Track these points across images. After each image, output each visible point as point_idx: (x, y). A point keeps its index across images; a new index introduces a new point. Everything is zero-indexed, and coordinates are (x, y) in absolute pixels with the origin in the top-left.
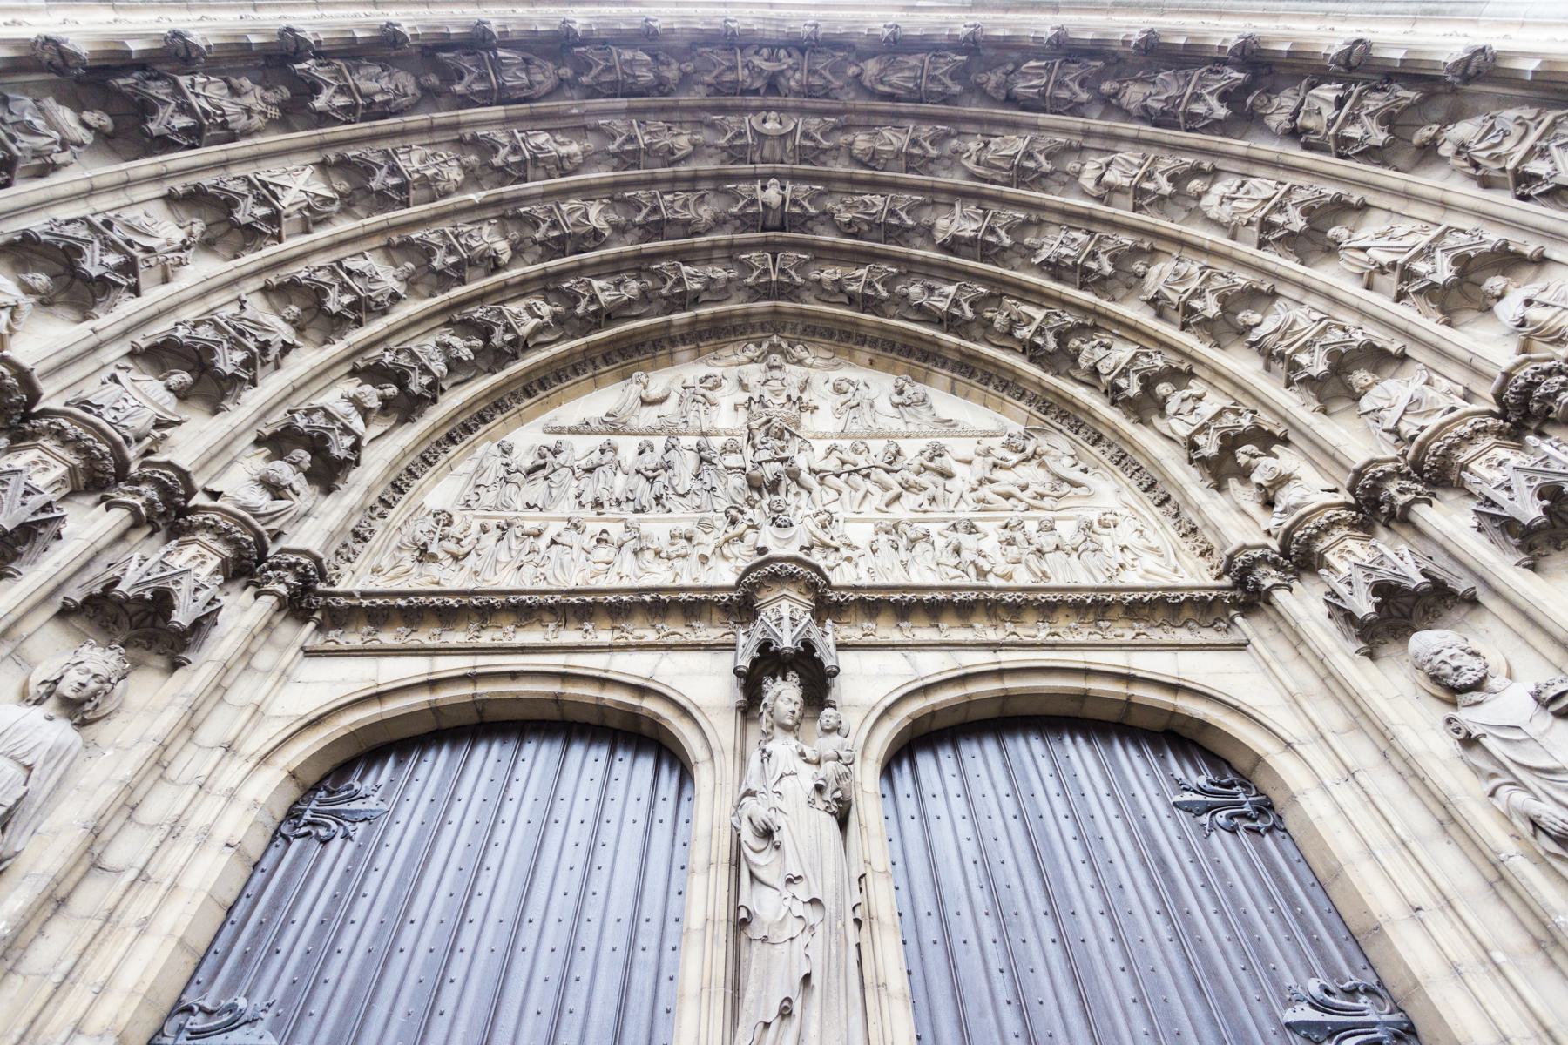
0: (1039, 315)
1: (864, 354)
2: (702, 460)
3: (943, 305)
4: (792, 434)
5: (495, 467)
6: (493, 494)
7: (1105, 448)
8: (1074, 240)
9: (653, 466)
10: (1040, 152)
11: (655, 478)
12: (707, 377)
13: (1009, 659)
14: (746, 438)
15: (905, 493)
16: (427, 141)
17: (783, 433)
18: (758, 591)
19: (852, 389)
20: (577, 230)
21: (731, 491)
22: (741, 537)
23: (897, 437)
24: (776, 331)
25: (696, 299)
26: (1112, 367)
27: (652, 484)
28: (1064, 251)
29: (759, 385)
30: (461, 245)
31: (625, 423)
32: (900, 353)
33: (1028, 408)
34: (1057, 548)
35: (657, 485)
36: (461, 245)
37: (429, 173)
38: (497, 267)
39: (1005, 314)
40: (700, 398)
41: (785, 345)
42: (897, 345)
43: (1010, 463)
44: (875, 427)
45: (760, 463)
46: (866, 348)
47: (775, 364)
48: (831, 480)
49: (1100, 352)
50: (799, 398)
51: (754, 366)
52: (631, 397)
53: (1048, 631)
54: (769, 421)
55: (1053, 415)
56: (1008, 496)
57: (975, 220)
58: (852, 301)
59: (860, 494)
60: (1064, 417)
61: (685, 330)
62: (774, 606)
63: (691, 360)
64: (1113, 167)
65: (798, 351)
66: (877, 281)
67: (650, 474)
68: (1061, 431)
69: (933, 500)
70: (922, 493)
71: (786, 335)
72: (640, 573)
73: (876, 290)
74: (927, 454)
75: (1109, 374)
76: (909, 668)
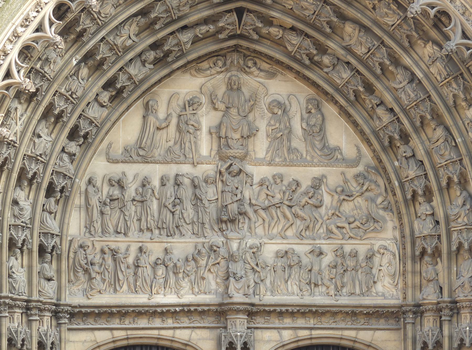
11: (174, 212)
13: (315, 333)
30: (73, 98)
34: (353, 269)
35: (177, 216)
41: (242, 62)
45: (226, 206)
48: (262, 213)
51: (221, 76)
53: (332, 321)
58: (288, 54)
62: (234, 320)
70: (304, 221)
74: (310, 195)
76: (279, 337)
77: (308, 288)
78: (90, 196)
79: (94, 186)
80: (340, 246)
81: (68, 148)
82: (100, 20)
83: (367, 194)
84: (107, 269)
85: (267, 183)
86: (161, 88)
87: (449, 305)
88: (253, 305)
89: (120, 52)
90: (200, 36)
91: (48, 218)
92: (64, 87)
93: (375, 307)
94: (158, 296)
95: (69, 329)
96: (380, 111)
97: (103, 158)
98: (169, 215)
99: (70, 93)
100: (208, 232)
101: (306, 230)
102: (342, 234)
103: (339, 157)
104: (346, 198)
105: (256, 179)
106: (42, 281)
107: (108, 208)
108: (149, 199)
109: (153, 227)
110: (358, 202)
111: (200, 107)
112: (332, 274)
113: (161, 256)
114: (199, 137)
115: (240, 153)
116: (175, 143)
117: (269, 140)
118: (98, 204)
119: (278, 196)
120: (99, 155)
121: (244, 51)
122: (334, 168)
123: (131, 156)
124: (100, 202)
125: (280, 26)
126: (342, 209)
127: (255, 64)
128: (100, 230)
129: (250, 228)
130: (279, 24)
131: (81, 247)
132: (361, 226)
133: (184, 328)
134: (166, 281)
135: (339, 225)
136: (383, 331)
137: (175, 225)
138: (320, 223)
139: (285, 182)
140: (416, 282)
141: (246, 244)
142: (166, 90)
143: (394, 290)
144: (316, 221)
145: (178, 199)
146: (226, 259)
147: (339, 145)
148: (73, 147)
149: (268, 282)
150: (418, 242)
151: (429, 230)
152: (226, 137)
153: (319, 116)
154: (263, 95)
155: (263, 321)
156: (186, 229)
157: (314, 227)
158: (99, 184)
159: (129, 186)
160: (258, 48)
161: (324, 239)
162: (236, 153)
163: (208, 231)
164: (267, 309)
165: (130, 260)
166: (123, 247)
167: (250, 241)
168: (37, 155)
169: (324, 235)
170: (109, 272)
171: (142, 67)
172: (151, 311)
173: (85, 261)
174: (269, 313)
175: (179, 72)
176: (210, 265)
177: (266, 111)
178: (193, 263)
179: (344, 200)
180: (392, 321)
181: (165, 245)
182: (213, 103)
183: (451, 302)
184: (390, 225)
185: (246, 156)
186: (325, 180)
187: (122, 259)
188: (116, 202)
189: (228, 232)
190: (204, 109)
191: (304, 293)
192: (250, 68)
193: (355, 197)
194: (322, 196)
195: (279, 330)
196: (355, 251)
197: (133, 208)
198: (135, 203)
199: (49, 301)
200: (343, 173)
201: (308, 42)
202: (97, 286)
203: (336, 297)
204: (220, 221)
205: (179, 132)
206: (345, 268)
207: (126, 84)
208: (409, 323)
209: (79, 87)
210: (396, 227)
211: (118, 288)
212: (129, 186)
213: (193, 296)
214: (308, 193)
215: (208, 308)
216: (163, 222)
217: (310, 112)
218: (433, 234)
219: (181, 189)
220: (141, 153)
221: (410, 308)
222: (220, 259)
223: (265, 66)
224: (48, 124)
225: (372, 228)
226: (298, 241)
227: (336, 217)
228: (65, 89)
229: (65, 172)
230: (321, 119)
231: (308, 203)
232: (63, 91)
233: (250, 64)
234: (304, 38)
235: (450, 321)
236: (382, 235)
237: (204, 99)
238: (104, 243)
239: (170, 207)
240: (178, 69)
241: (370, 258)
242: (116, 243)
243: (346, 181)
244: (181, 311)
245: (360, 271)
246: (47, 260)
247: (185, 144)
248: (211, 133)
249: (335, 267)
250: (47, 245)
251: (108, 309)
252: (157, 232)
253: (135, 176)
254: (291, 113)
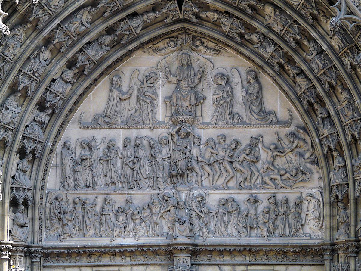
1: (233, 52)
5: (68, 161)
6: (72, 179)
30: (35, 76)
34: (283, 214)
35: (135, 172)
36: (35, 76)
48: (207, 168)
51: (175, 54)
52: (115, 101)
59: (216, 177)
70: (243, 174)
74: (247, 152)
77: (245, 230)
78: (64, 157)
79: (68, 149)
80: (273, 194)
81: (37, 117)
82: (50, 10)
83: (297, 150)
84: (77, 217)
85: (212, 143)
86: (124, 66)
87: (353, 243)
88: (196, 245)
89: (75, 37)
90: (148, 21)
91: (21, 175)
92: (28, 67)
93: (300, 246)
94: (119, 238)
95: (45, 267)
96: (299, 80)
97: (76, 125)
98: (130, 172)
99: (32, 72)
100: (162, 185)
102: (275, 184)
103: (274, 119)
104: (278, 154)
105: (203, 140)
106: (16, 226)
107: (79, 166)
108: (113, 158)
109: (116, 181)
110: (290, 157)
111: (157, 81)
112: (265, 218)
113: (123, 205)
114: (156, 106)
115: (188, 119)
116: (136, 111)
117: (215, 106)
118: (71, 163)
119: (221, 153)
120: (73, 123)
121: (192, 33)
122: (270, 129)
123: (98, 123)
124: (74, 162)
125: (216, 10)
126: (276, 163)
127: (202, 43)
128: (72, 185)
129: (197, 181)
130: (215, 9)
131: (56, 199)
132: (291, 178)
133: (139, 265)
134: (125, 227)
135: (272, 176)
136: (310, 267)
138: (256, 176)
139: (228, 142)
140: (334, 224)
141: (193, 194)
142: (129, 67)
143: (319, 232)
144: (253, 174)
145: (137, 158)
146: (176, 207)
147: (274, 109)
148: (43, 117)
149: (212, 226)
150: (334, 190)
151: (341, 179)
152: (176, 105)
153: (256, 85)
154: (210, 69)
155: (206, 258)
156: (144, 182)
157: (250, 179)
158: (72, 146)
159: (98, 148)
160: (200, 29)
161: (259, 189)
163: (162, 184)
164: (208, 248)
165: (98, 209)
166: (91, 198)
167: (196, 192)
168: (5, 124)
169: (259, 186)
171: (100, 49)
172: (111, 251)
173: (59, 210)
174: (211, 252)
175: (138, 53)
176: (162, 212)
177: (212, 82)
178: (148, 211)
179: (277, 155)
180: (317, 258)
181: (126, 196)
182: (168, 78)
183: (356, 241)
184: (316, 176)
185: (194, 121)
186: (261, 139)
187: (90, 209)
188: (86, 161)
189: (177, 185)
190: (160, 82)
191: (241, 235)
192: (198, 46)
193: (286, 153)
194: (259, 153)
195: (220, 266)
196: (285, 199)
197: (101, 166)
198: (102, 162)
199: (20, 243)
200: (277, 133)
201: (238, 22)
202: (68, 231)
203: (268, 238)
204: (171, 176)
205: (139, 102)
206: (277, 213)
207: (85, 63)
208: (327, 259)
209: (40, 67)
210: (321, 178)
211: (85, 232)
212: (98, 148)
213: (148, 238)
214: (246, 150)
215: (158, 248)
216: (124, 177)
217: (249, 82)
218: (344, 183)
219: (139, 149)
220: (107, 120)
221: (327, 247)
222: (170, 207)
223: (211, 45)
224: (16, 97)
225: (301, 179)
226: (238, 191)
227: (270, 170)
228: (29, 69)
229: (34, 138)
230: (257, 87)
232: (26, 70)
233: (198, 43)
234: (234, 20)
235: (355, 257)
236: (309, 185)
237: (160, 74)
238: (76, 195)
239: (131, 164)
240: (137, 48)
241: (299, 205)
242: (86, 195)
243: (279, 139)
244: (136, 251)
245: (290, 217)
246: (20, 210)
247: (143, 112)
248: (166, 103)
249: (268, 212)
250: (18, 197)
251: (75, 250)
252: (120, 185)
253: (103, 139)
254: (233, 84)
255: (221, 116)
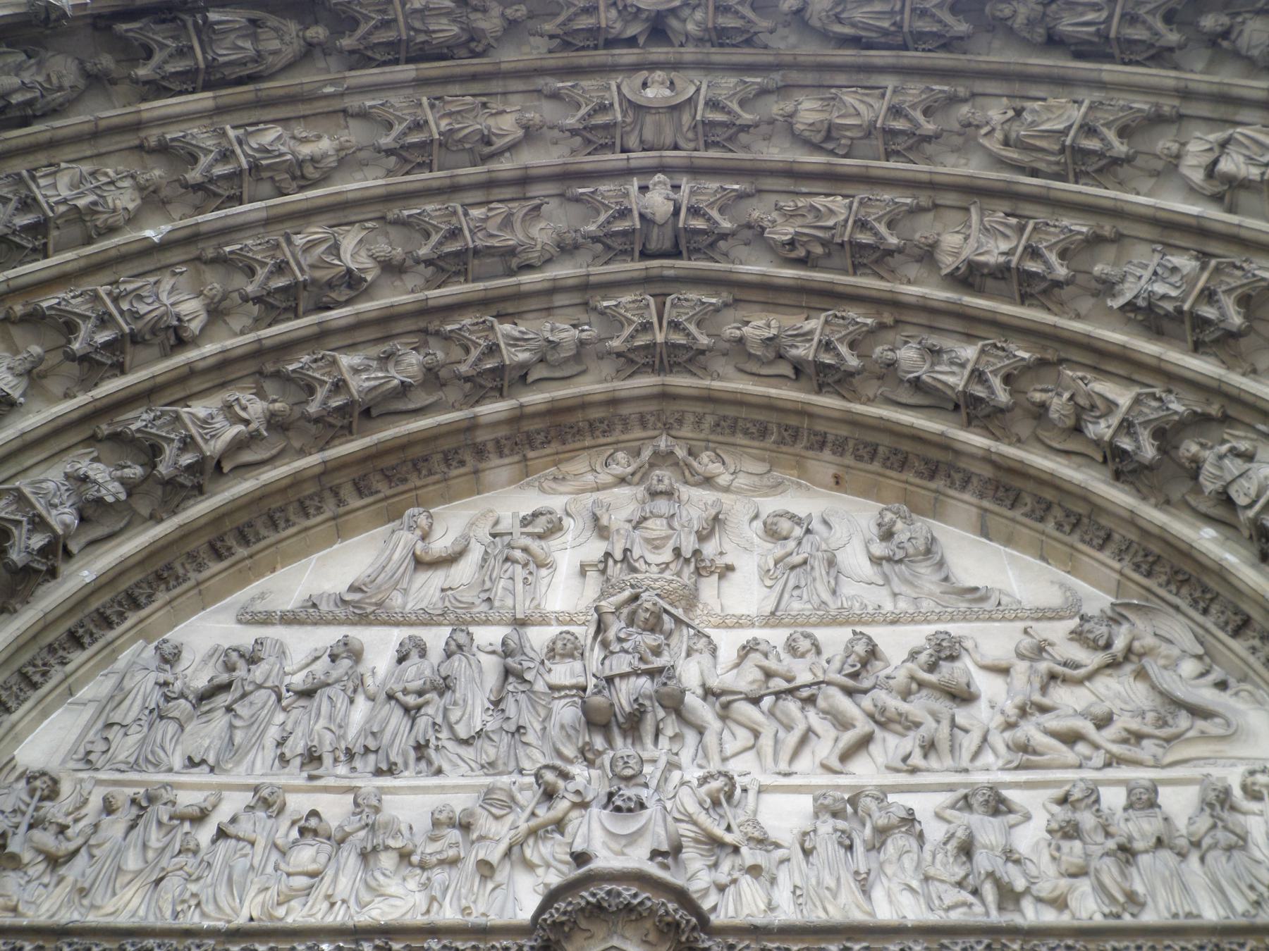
0: (1123, 397)
1: (824, 465)
2: (507, 672)
3: (956, 380)
4: (678, 621)
5: (144, 686)
6: (134, 739)
7: (1257, 642)
8: (1174, 270)
9: (417, 684)
10: (1108, 125)
11: (419, 708)
12: (535, 515)
14: (592, 630)
15: (879, 733)
16: (88, 153)
17: (659, 618)
18: (568, 937)
19: (798, 532)
20: (318, 274)
21: (554, 731)
22: (559, 825)
23: (873, 622)
24: (667, 427)
25: (524, 378)
26: (1253, 492)
27: (414, 720)
28: (1160, 288)
29: (629, 526)
30: (122, 312)
31: (379, 604)
32: (886, 463)
33: (1117, 565)
34: (1159, 842)
35: (422, 722)
37: (81, 203)
38: (178, 338)
39: (1066, 395)
40: (518, 554)
42: (881, 450)
43: (1081, 672)
44: (833, 605)
45: (610, 680)
46: (827, 454)
47: (661, 487)
48: (744, 709)
49: (1233, 466)
50: (696, 553)
51: (625, 491)
52: (396, 556)
54: (636, 598)
55: (1163, 578)
56: (1071, 738)
57: (1006, 236)
59: (792, 739)
60: (1183, 582)
61: (502, 432)
63: (511, 482)
64: (1231, 148)
65: (706, 463)
66: (840, 340)
67: (411, 700)
68: (1177, 608)
69: (929, 747)
70: (912, 734)
71: (682, 433)
72: (366, 897)
73: (838, 355)
74: (923, 658)
75: (1250, 506)
101: (925, 756)
108: (337, 681)
110: (1107, 687)
114: (546, 581)
122: (997, 624)
129: (706, 756)
137: (412, 742)
154: (747, 518)
162: (656, 580)
170: (92, 856)
177: (757, 540)
179: (1053, 677)
187: (165, 819)
190: (569, 537)
212: (287, 669)
231: (922, 684)
255: (796, 593)
